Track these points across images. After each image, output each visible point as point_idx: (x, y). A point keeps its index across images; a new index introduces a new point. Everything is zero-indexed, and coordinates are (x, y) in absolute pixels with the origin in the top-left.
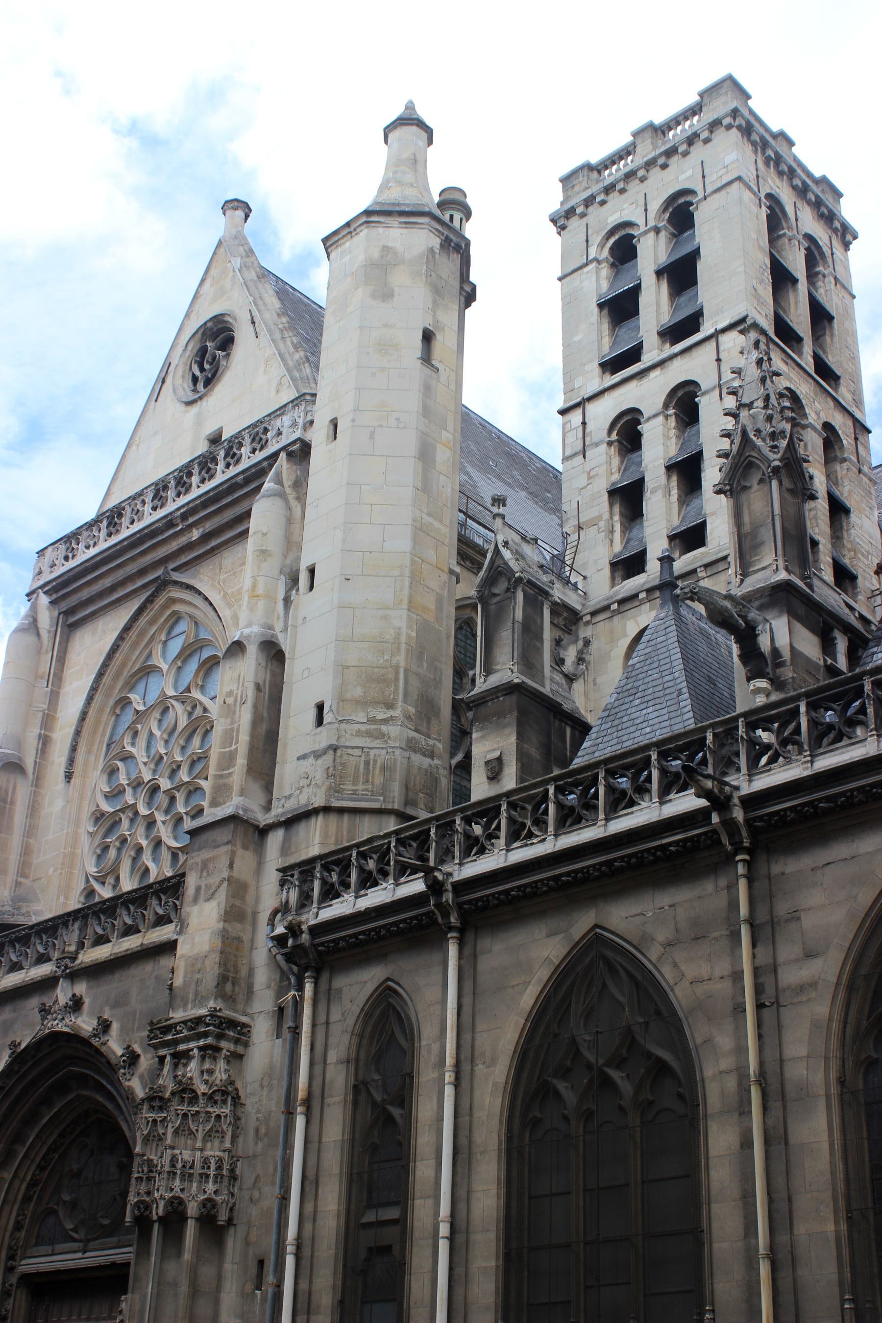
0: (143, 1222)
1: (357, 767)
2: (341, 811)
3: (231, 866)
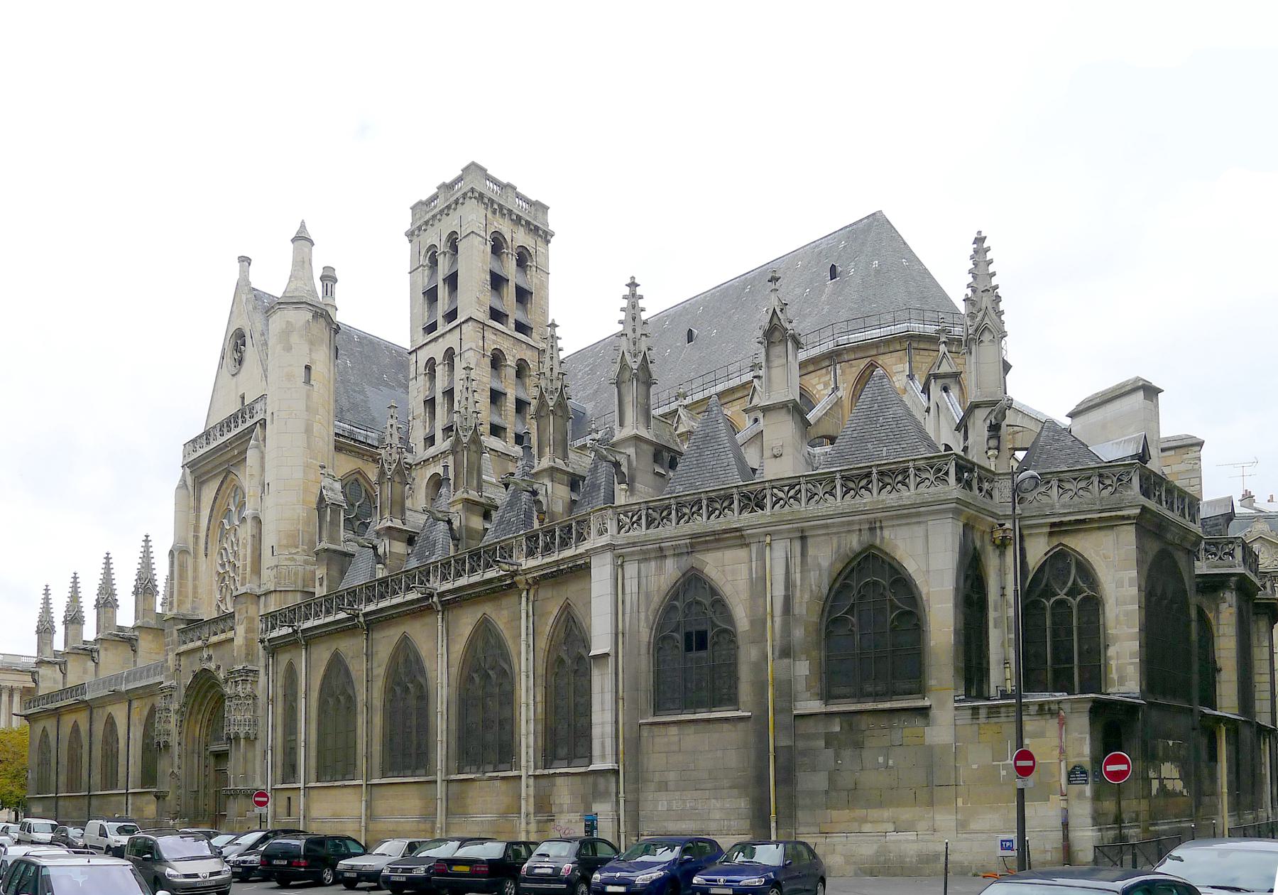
0: (229, 738)
1: (285, 574)
2: (281, 591)
3: (247, 612)
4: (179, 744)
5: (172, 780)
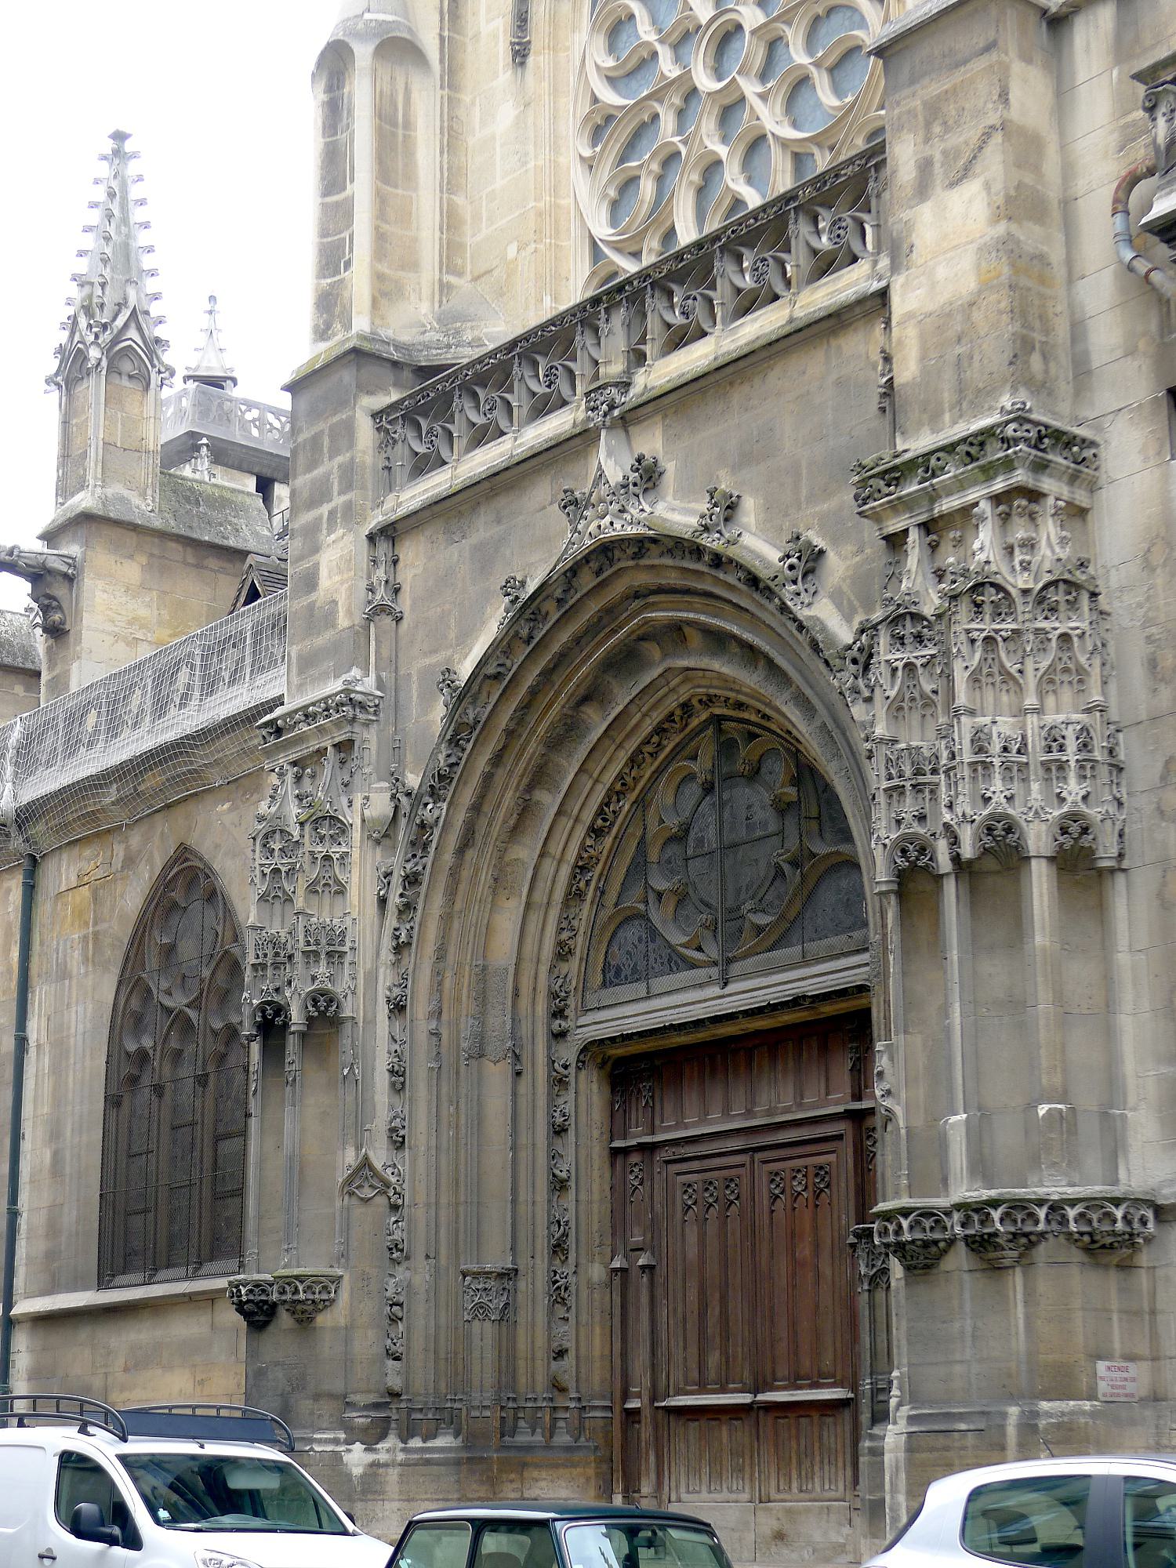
4: (398, 1008)
5: (359, 1211)
